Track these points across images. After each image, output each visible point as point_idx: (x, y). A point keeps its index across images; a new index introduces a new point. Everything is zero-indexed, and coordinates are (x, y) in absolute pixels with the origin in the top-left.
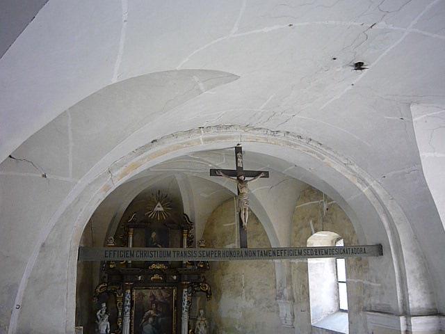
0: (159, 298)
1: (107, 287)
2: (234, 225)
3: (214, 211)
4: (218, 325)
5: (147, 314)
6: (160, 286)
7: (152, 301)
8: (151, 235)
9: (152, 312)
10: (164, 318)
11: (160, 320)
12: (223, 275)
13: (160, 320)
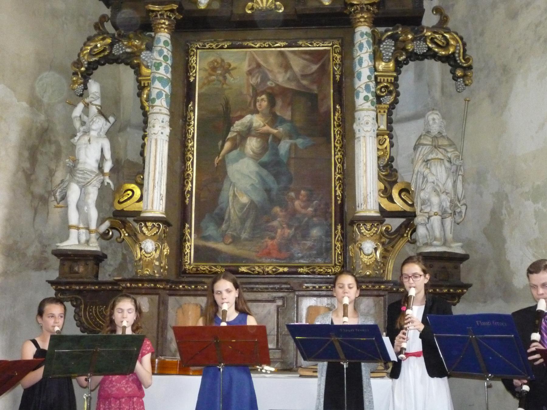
0: (281, 78)
1: (111, 45)
4: (508, 188)
5: (238, 126)
6: (279, 40)
9: (257, 121)
10: (300, 141)
11: (284, 146)
12: (513, 15)
13: (284, 146)
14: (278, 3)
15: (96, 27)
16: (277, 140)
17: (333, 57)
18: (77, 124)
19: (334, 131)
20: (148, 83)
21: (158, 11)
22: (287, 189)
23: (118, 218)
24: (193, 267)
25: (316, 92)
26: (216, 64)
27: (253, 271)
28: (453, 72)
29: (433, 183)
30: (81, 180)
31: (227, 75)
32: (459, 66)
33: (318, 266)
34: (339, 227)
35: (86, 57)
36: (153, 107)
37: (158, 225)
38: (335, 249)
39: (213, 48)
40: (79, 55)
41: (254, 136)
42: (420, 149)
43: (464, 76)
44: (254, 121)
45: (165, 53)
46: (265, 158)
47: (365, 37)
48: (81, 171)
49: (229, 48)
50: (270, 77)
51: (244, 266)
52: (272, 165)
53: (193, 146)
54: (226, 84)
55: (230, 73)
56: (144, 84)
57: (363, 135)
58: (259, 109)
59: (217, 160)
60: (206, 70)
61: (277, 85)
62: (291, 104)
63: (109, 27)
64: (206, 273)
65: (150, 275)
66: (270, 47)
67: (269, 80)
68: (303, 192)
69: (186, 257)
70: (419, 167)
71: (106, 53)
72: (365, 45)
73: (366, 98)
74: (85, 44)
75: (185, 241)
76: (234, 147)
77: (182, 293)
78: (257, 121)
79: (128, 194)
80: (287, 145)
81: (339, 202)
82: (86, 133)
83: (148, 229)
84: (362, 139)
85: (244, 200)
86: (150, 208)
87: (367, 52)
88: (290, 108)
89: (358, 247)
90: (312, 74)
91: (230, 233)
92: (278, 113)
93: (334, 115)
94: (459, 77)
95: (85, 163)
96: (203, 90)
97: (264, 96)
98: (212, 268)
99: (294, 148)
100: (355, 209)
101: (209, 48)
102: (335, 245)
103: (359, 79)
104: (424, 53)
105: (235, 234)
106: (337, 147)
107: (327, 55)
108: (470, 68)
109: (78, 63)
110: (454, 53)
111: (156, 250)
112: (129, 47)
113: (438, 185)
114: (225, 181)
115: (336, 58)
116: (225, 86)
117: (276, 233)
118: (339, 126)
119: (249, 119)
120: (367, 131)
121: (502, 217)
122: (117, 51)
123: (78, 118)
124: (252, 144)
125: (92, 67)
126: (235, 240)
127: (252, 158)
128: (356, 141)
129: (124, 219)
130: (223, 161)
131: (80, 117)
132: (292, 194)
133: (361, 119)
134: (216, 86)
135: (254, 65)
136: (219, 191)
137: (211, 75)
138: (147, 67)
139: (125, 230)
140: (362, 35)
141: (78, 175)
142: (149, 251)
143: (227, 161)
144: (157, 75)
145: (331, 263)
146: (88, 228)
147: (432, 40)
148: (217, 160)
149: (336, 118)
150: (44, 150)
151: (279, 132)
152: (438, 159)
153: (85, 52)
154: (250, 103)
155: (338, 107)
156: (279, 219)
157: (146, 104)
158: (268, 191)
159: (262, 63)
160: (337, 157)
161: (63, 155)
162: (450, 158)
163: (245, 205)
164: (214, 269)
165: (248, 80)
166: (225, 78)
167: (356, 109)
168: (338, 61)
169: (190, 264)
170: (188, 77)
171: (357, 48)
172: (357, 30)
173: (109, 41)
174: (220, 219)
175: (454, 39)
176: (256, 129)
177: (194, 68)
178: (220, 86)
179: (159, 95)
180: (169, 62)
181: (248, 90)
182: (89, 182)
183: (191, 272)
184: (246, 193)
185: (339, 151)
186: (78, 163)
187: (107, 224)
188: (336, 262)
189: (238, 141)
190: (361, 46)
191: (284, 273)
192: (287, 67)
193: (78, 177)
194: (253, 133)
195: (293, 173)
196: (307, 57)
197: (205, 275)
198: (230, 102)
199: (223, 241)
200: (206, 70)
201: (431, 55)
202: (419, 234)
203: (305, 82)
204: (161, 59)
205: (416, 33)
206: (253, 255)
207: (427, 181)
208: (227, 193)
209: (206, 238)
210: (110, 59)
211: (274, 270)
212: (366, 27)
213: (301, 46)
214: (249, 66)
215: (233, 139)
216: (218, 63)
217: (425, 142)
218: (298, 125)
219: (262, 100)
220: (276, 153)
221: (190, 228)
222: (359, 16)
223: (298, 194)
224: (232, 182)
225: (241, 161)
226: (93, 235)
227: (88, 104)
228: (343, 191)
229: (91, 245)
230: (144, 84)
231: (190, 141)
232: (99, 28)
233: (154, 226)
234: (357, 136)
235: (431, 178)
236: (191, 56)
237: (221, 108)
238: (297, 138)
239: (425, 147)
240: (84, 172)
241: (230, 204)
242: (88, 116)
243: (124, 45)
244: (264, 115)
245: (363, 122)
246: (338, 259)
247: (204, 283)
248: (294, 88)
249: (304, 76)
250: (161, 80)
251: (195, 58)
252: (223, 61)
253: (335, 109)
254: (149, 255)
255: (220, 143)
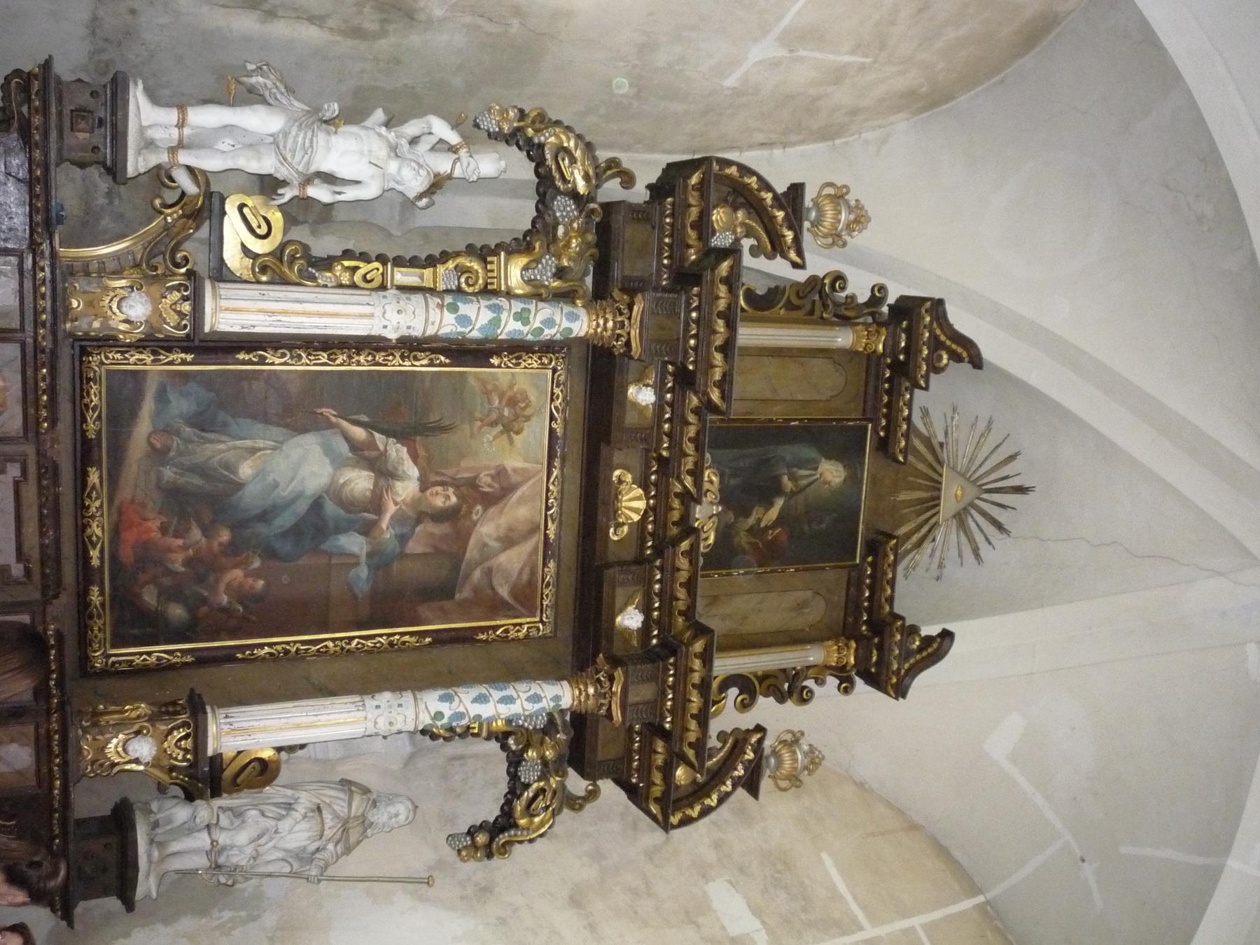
0: (488, 528)
1: (574, 195)
2: (861, 928)
3: (861, 785)
5: (397, 452)
7: (472, 484)
8: (829, 457)
9: (406, 489)
10: (363, 572)
11: (354, 543)
13: (354, 543)
14: (626, 528)
15: (613, 163)
16: (367, 529)
17: (521, 625)
18: (412, 128)
19: (381, 636)
20: (492, 271)
21: (629, 318)
22: (270, 554)
23: (207, 202)
24: (95, 372)
25: (457, 596)
26: (523, 405)
27: (89, 496)
28: (483, 827)
29: (276, 832)
30: (290, 141)
31: (500, 428)
32: (494, 836)
33: (104, 624)
34: (189, 659)
35: (552, 139)
36: (441, 307)
37: (186, 326)
38: (141, 654)
39: (552, 400)
40: (558, 123)
41: (376, 485)
42: (342, 795)
43: (474, 846)
44: (406, 483)
45: (547, 331)
46: (331, 508)
47: (552, 704)
48: (311, 142)
49: (552, 431)
50: (492, 510)
51: (101, 477)
52: (315, 524)
53: (359, 363)
54: (480, 428)
55: (502, 432)
56: (492, 263)
57: (370, 716)
58: (428, 492)
59: (328, 412)
60: (511, 386)
61: (475, 524)
62: (438, 551)
63: (612, 190)
64: (82, 397)
65: (68, 308)
66: (548, 508)
67: (485, 510)
68: (261, 583)
69: (118, 356)
70: (305, 800)
71: (559, 184)
72: (537, 706)
73: (439, 715)
74: (579, 137)
75: (154, 353)
76: (354, 446)
77: (30, 373)
78: (406, 489)
79: (259, 227)
80: (355, 550)
81: (239, 656)
82: (394, 150)
83: (175, 303)
84: (362, 714)
85: (246, 470)
86: (224, 304)
87: (524, 710)
88: (428, 550)
89: (142, 728)
90: (493, 589)
91: (175, 444)
92: (418, 529)
93: (411, 634)
94: (473, 839)
95: (328, 149)
96: (472, 381)
97: (454, 499)
98: (94, 410)
99: (351, 561)
100: (221, 706)
101: (553, 394)
102: (149, 654)
103: (475, 700)
104: (519, 778)
105: (172, 454)
106: (349, 644)
107: (523, 611)
108: (490, 856)
109: (543, 121)
110: (516, 826)
111: (127, 321)
112: (566, 234)
113: (271, 839)
114: (284, 431)
115: (518, 631)
116: (479, 423)
117: (176, 537)
118: (391, 644)
119: (410, 473)
120: (376, 723)
121: (215, 914)
122: (563, 208)
123: (426, 131)
124: (360, 482)
125: (535, 152)
126: (158, 455)
127: (333, 482)
128: (357, 698)
129: (206, 214)
130: (331, 426)
131: (430, 133)
132: (257, 564)
133: (400, 710)
134: (479, 408)
135: (515, 478)
136: (266, 420)
137: (501, 396)
138: (526, 268)
139: (180, 217)
140: (557, 698)
141: (302, 136)
142: (124, 309)
143: (328, 433)
144: (504, 316)
145: (114, 646)
146: (181, 145)
147: (542, 791)
148: (328, 412)
149: (406, 638)
150: (367, 9)
151: (382, 532)
152: (323, 830)
153: (564, 138)
154: (443, 475)
155: (428, 640)
156: (204, 539)
157: (451, 265)
158: (265, 516)
159: (519, 493)
160: (331, 644)
161: (356, 42)
162: (324, 849)
163: (235, 473)
164: (91, 416)
165: (487, 468)
166: (493, 424)
167: (419, 695)
168: (512, 634)
169: (102, 363)
170: (499, 355)
171: (532, 692)
172: (565, 683)
173: (581, 187)
174: (204, 423)
175: (542, 824)
176: (389, 488)
177: (518, 364)
178: (478, 415)
179: (464, 320)
180: (530, 337)
181: (467, 469)
182: (285, 159)
183: (85, 365)
184: (260, 474)
185: (342, 649)
186: (329, 133)
187: (191, 188)
188: (113, 659)
189: (366, 453)
190: (536, 698)
191: (87, 558)
192: (509, 541)
193: (297, 136)
194: (382, 482)
195: (302, 562)
196: (525, 577)
197: (78, 398)
198: (445, 436)
199: (155, 432)
200: (511, 386)
201: (516, 787)
202: (174, 811)
203: (477, 574)
204: (537, 324)
205: (559, 759)
206: (125, 493)
207: (280, 818)
208: (263, 437)
209: (162, 397)
210: (546, 185)
211: (94, 538)
212: (570, 702)
213: (545, 565)
214: (515, 470)
215: (372, 445)
216: (525, 408)
217: (354, 805)
218: (396, 566)
219: (448, 497)
220: (340, 529)
221: (184, 362)
222: (591, 690)
223: (256, 574)
224: (282, 443)
225: (327, 461)
226: (164, 158)
227: (455, 152)
228: (263, 659)
229: (141, 159)
230: (492, 263)
231: (370, 358)
232: (609, 168)
233: (181, 314)
234: (370, 702)
235: (284, 825)
236: (540, 358)
237: (434, 417)
238: (369, 567)
239: (345, 805)
240: (309, 149)
241: (238, 443)
242: (433, 149)
243: (572, 222)
244: (415, 503)
245: (394, 714)
246: (120, 663)
247: (54, 421)
248: (468, 555)
249: (489, 573)
250: (495, 322)
251: (535, 365)
252: (528, 418)
253: (422, 634)
254: (114, 307)
255: (364, 418)
